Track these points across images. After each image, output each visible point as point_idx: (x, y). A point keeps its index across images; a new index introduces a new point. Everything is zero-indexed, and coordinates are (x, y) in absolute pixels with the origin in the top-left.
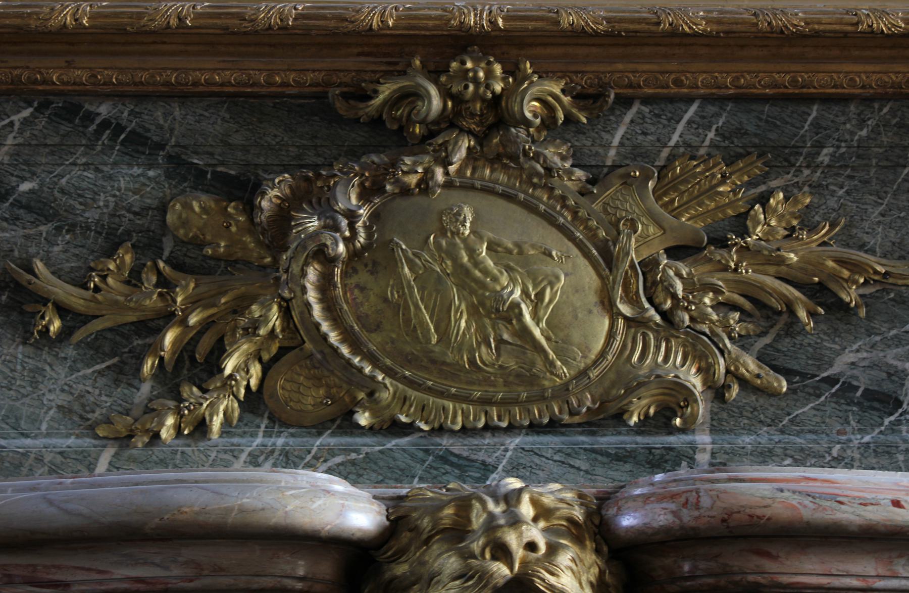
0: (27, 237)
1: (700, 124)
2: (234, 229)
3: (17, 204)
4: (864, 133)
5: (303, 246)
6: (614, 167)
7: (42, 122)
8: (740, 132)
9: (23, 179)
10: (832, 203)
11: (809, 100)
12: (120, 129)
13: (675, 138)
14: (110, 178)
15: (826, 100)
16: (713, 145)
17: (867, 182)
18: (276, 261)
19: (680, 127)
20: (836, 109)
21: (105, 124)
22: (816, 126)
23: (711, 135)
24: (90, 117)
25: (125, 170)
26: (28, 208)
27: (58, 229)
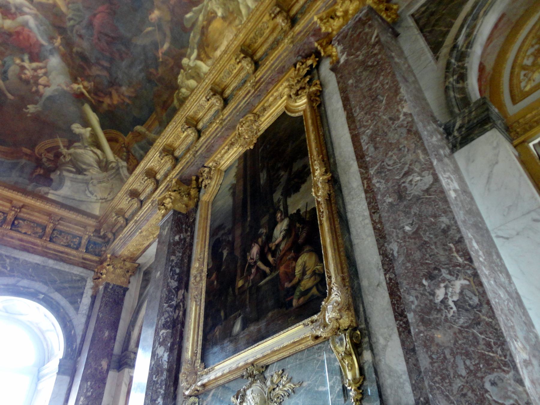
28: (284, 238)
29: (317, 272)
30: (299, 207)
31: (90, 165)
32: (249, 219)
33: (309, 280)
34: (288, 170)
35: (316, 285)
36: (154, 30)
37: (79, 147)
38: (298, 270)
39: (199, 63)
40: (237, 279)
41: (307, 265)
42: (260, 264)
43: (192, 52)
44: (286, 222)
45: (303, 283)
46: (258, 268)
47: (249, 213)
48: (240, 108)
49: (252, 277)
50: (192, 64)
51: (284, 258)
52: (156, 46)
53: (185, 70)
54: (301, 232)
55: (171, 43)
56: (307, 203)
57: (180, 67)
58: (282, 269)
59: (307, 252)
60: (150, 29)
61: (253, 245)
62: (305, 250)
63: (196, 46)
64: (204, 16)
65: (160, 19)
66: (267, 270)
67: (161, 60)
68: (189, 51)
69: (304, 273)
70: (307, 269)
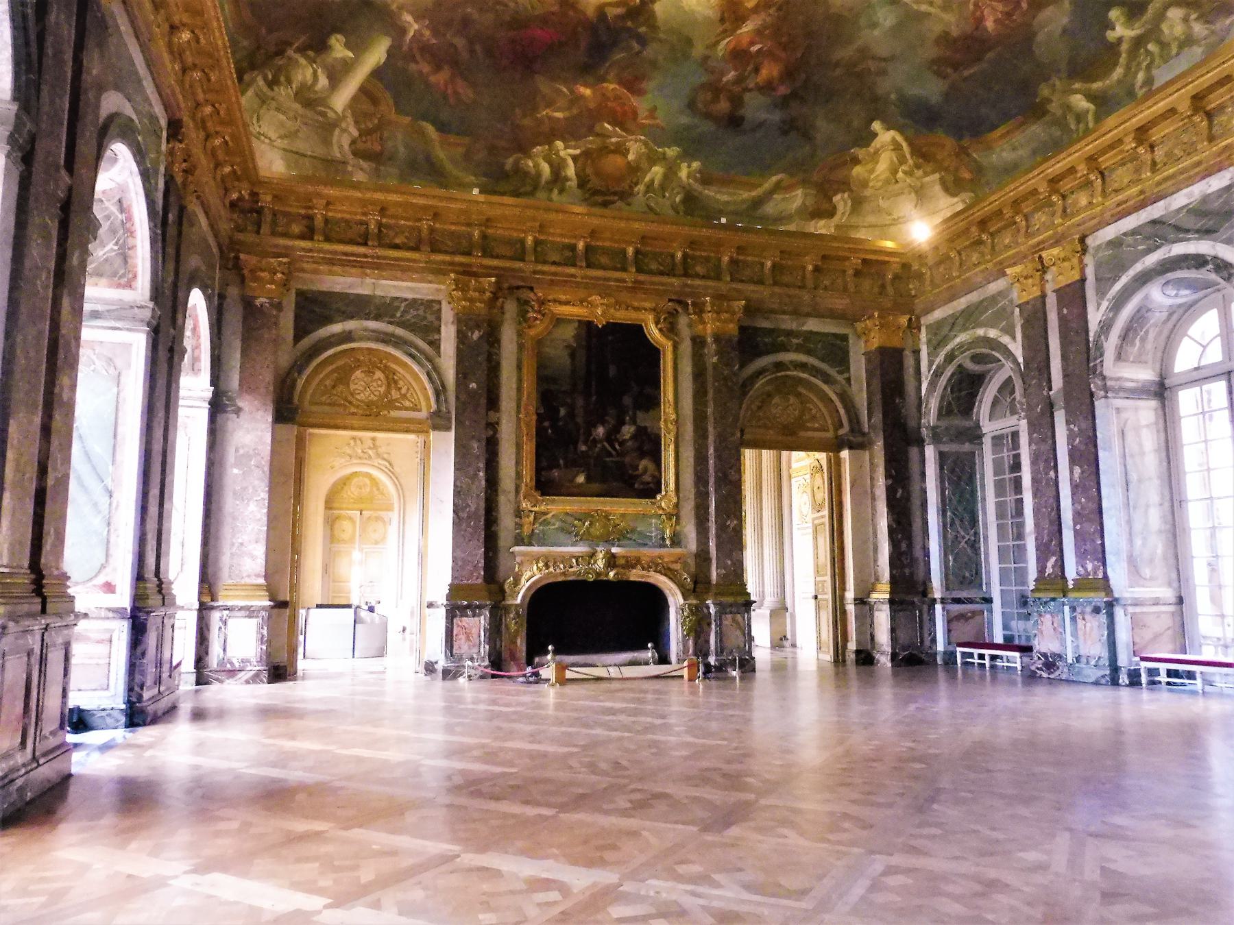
28: (631, 438)
31: (289, 82)
36: (565, 95)
37: (307, 58)
38: (640, 467)
39: (570, 162)
42: (605, 444)
43: (575, 148)
44: (633, 429)
46: (603, 446)
49: (597, 449)
50: (562, 153)
52: (550, 104)
53: (550, 150)
55: (566, 119)
57: (550, 143)
58: (627, 460)
60: (565, 90)
63: (583, 149)
64: (618, 143)
65: (582, 97)
66: (614, 453)
67: (538, 115)
68: (573, 143)
69: (645, 470)
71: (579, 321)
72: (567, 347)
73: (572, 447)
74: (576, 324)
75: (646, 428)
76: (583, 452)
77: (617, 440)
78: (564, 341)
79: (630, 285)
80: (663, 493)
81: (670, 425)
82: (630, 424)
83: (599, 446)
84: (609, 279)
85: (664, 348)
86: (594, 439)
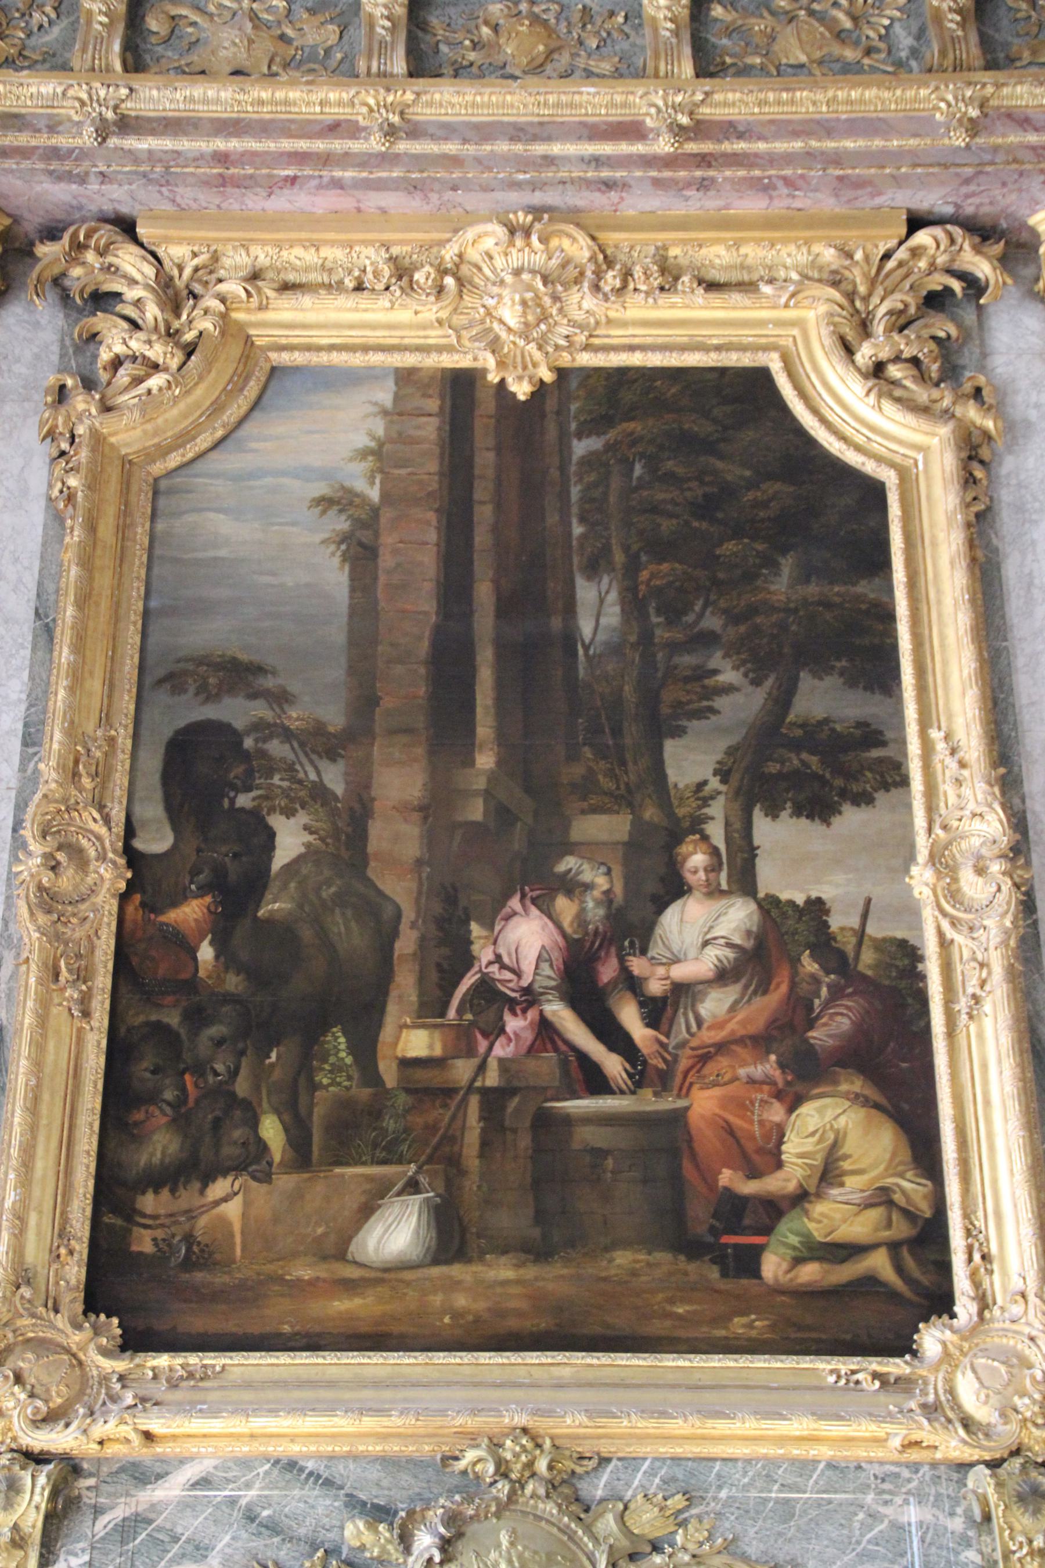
0: (266, 1546)
1: (652, 1473)
2: (382, 1541)
3: (261, 1525)
4: (746, 1480)
5: (421, 1554)
6: (602, 1500)
7: (276, 1472)
8: (674, 1479)
9: (264, 1508)
10: (727, 1525)
11: (714, 1460)
12: (319, 1476)
13: (636, 1483)
14: (313, 1507)
15: (724, 1460)
16: (659, 1487)
17: (747, 1512)
18: (405, 1562)
19: (640, 1475)
20: (730, 1464)
21: (311, 1474)
22: (719, 1476)
23: (657, 1480)
24: (302, 1470)
25: (321, 1501)
26: (267, 1527)
27: (283, 1540)
28: (723, 976)
29: (897, 1197)
30: (826, 892)
32: (485, 760)
33: (857, 1214)
34: (769, 682)
35: (894, 1247)
38: (793, 1147)
40: (392, 1009)
41: (847, 1148)
45: (819, 1208)
46: (546, 1028)
47: (485, 728)
48: (549, 161)
49: (501, 1050)
51: (723, 1063)
54: (826, 1006)
56: (868, 901)
59: (846, 1096)
61: (515, 903)
62: (844, 1087)
66: (613, 1065)
70: (846, 1165)
71: (405, 377)
72: (325, 503)
73: (338, 1041)
74: (385, 395)
75: (817, 907)
76: (407, 1064)
77: (633, 984)
78: (305, 473)
79: (664, 145)
80: (965, 1308)
81: (972, 886)
82: (714, 892)
83: (514, 1024)
84: (541, 131)
85: (904, 474)
86: (486, 989)
